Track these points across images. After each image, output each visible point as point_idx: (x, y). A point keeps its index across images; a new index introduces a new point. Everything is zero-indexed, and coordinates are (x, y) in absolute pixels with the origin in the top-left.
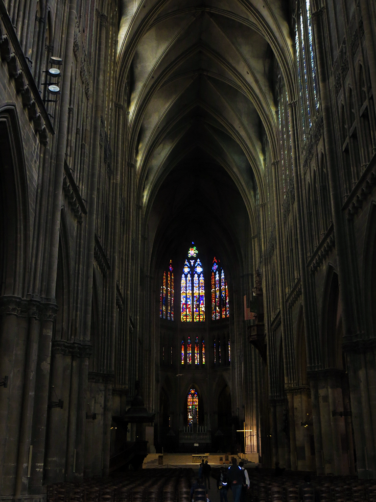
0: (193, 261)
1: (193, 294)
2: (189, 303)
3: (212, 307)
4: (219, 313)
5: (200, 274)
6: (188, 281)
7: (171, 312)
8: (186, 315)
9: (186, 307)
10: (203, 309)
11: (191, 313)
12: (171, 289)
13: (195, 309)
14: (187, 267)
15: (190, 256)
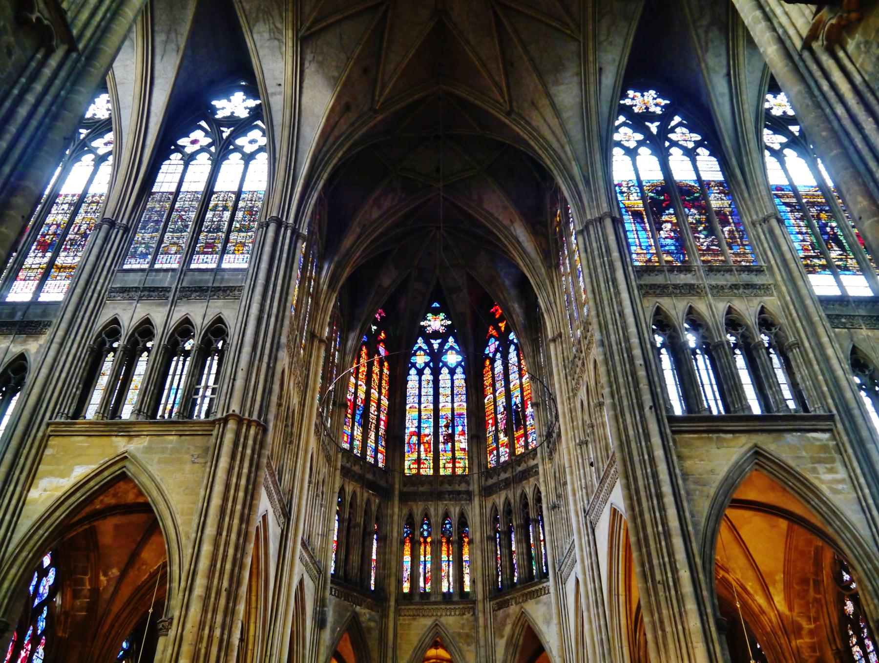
0: (439, 341)
1: (436, 410)
2: (427, 432)
3: (486, 439)
4: (507, 446)
5: (456, 367)
6: (424, 383)
7: (377, 447)
8: (418, 461)
9: (419, 440)
10: (464, 445)
11: (431, 455)
12: (380, 393)
13: (441, 446)
14: (422, 353)
15: (429, 330)
